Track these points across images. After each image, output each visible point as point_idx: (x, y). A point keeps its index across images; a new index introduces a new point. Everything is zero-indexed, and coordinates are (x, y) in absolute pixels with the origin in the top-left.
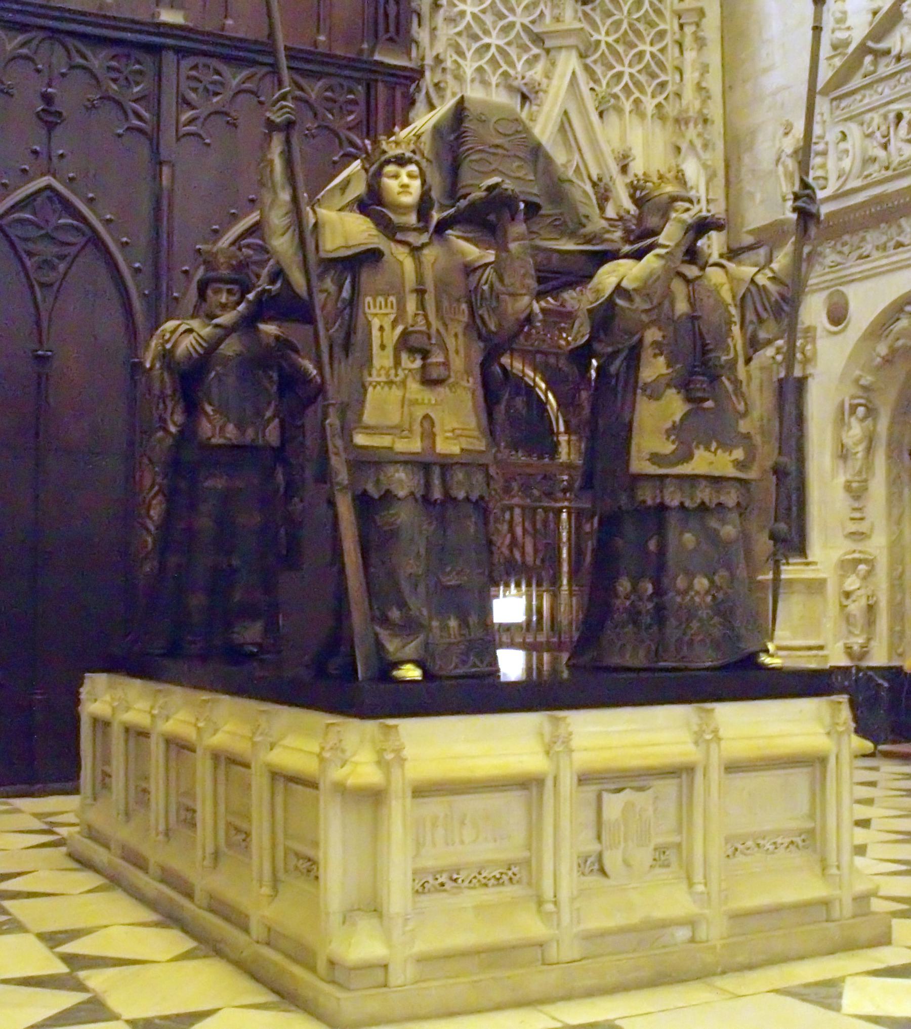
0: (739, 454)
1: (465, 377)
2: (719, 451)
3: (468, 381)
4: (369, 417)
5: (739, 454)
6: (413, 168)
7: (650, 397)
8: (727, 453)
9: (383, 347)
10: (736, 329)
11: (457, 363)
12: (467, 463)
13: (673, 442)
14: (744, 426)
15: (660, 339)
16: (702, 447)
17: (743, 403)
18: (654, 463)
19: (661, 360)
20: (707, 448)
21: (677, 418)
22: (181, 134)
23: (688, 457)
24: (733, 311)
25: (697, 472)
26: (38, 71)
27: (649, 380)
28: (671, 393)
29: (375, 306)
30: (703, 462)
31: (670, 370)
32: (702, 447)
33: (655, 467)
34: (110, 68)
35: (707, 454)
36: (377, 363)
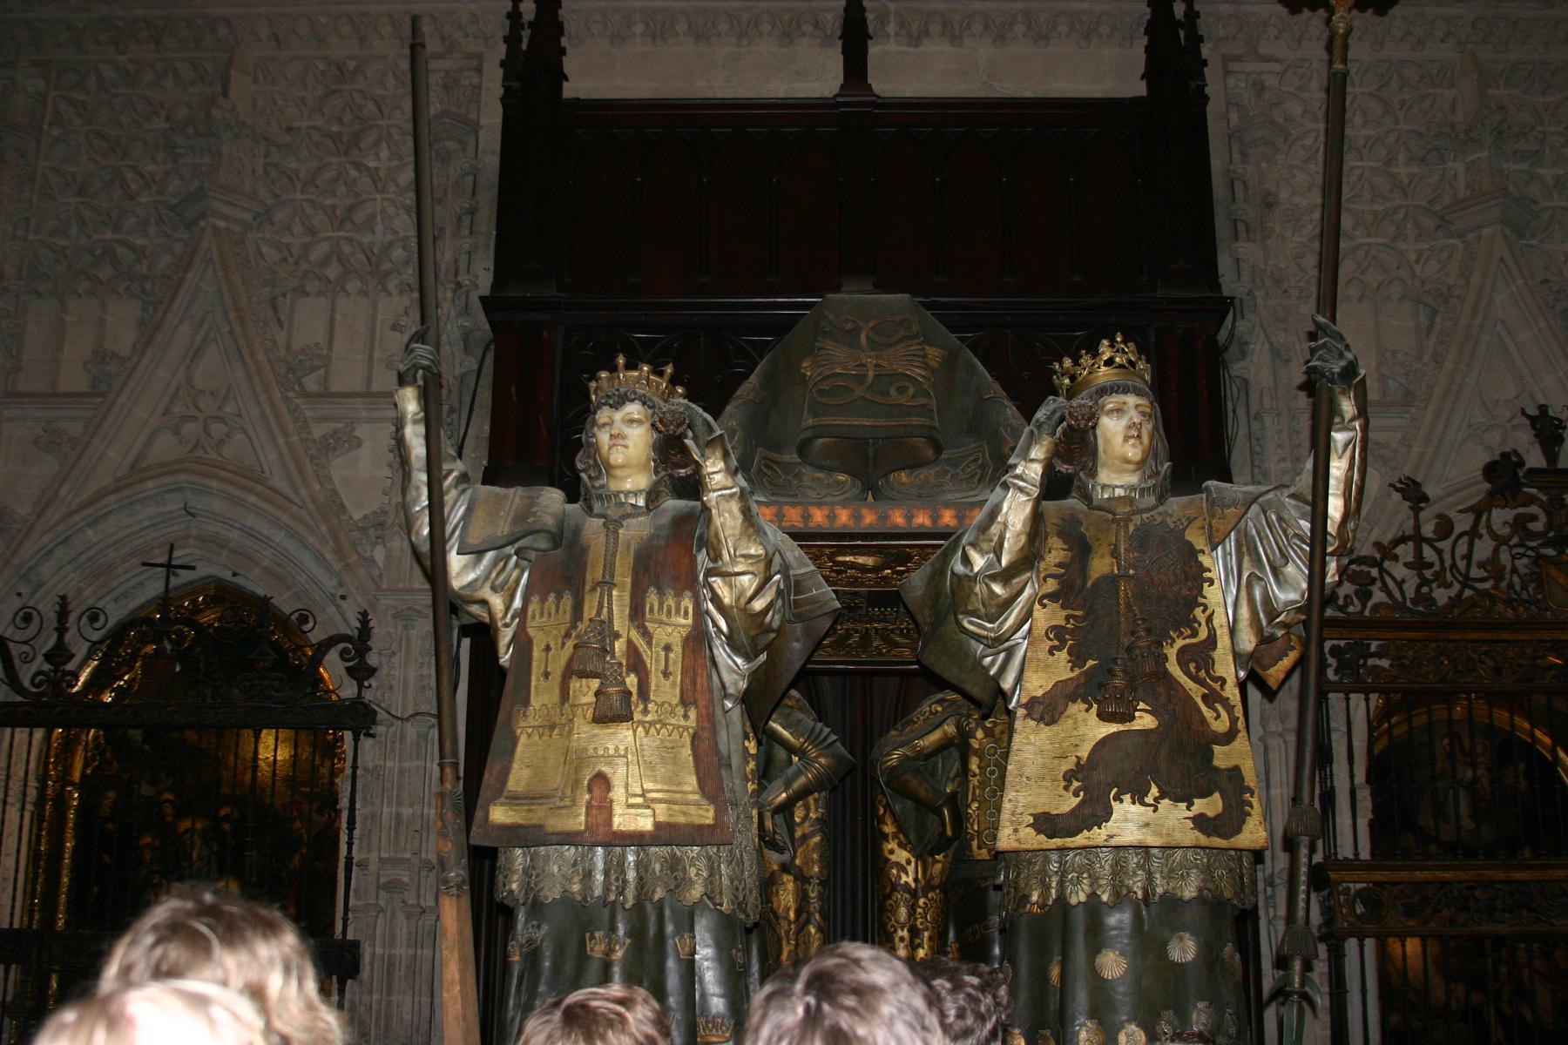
0: (1210, 805)
1: (680, 711)
2: (1166, 802)
3: (686, 716)
4: (519, 777)
5: (1210, 805)
7: (1040, 720)
8: (1183, 805)
9: (546, 675)
13: (1076, 794)
14: (1222, 757)
15: (1063, 623)
16: (1127, 798)
17: (1224, 714)
18: (1039, 831)
19: (1063, 655)
20: (1139, 797)
21: (1084, 753)
27: (1039, 693)
28: (1076, 708)
29: (542, 615)
31: (1077, 672)
32: (1127, 798)
33: (1042, 837)
35: (1137, 809)
36: (535, 702)
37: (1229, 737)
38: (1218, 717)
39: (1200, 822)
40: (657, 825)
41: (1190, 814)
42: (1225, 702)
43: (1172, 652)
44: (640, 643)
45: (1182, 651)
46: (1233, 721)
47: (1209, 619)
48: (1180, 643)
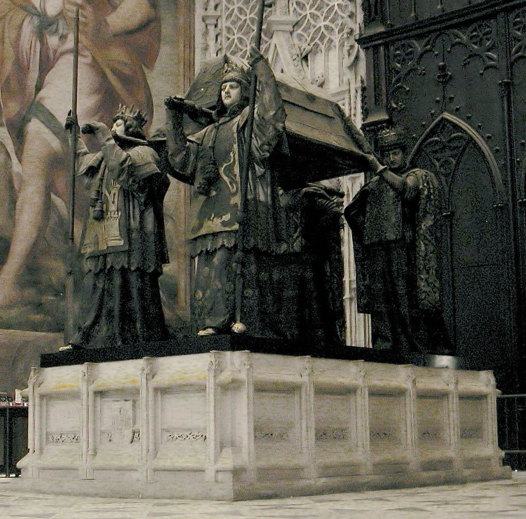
0: (227, 217)
3: (118, 214)
5: (227, 217)
6: (119, 121)
10: (236, 146)
11: (113, 208)
12: (116, 252)
17: (235, 187)
20: (209, 219)
22: (513, 58)
23: (201, 226)
24: (235, 135)
25: (204, 233)
26: (436, 55)
30: (214, 224)
34: (471, 38)
37: (235, 194)
38: (233, 188)
39: (224, 224)
40: (108, 247)
41: (222, 220)
42: (236, 183)
43: (222, 170)
44: (108, 194)
45: (225, 167)
46: (237, 189)
47: (234, 156)
48: (225, 165)
